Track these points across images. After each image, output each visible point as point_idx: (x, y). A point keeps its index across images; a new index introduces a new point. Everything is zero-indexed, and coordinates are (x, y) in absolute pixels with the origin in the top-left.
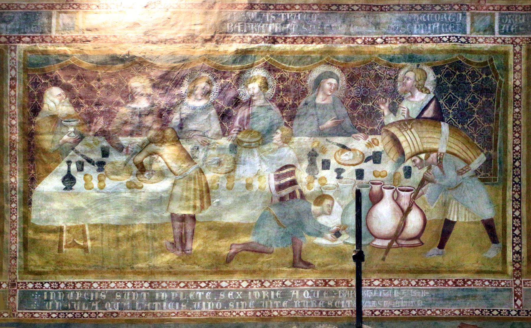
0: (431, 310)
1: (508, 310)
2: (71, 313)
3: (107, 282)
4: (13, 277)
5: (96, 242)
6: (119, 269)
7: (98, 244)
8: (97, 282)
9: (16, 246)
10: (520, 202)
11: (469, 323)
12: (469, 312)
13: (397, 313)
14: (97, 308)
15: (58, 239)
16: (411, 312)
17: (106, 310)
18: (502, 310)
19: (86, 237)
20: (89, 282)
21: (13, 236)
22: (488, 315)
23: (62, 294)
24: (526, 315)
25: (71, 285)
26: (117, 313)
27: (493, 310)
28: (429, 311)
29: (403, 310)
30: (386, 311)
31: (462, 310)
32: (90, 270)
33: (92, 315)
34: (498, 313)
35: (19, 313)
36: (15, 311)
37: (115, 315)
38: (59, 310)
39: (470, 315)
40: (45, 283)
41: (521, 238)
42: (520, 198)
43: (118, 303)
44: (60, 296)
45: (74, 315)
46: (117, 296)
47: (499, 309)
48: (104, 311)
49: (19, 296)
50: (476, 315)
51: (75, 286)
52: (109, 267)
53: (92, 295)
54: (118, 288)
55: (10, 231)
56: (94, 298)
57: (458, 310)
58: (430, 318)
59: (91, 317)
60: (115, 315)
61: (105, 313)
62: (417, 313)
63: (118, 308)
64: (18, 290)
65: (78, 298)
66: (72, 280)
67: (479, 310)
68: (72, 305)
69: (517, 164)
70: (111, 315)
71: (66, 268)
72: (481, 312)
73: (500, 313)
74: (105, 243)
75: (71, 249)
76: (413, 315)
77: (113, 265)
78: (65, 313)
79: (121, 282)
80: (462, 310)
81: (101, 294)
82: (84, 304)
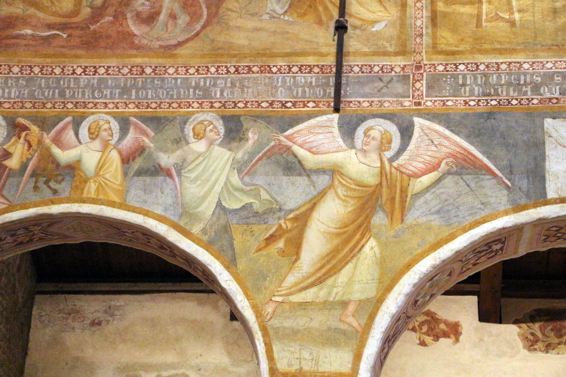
2: (496, 100)
3: (541, 62)
4: (418, 58)
5: (525, 14)
6: (557, 46)
7: (528, 17)
8: (528, 62)
9: (422, 21)
14: (529, 93)
15: (476, 12)
17: (541, 95)
19: (513, 9)
20: (518, 63)
21: (419, 9)
23: (482, 77)
25: (493, 67)
26: (557, 99)
32: (519, 47)
33: (523, 102)
35: (427, 101)
36: (422, 98)
37: (554, 101)
38: (479, 96)
40: (460, 64)
43: (558, 87)
44: (479, 80)
45: (499, 102)
46: (556, 78)
48: (539, 97)
49: (426, 80)
51: (498, 67)
52: (544, 44)
53: (522, 78)
54: (557, 68)
55: (415, 3)
56: (525, 82)
59: (522, 104)
60: (554, 101)
61: (541, 99)
63: (558, 93)
64: (425, 74)
65: (503, 82)
66: (494, 61)
68: (496, 90)
70: (550, 101)
71: (487, 46)
74: (538, 16)
75: (493, 23)
77: (550, 42)
78: (486, 100)
79: (561, 61)
81: (535, 77)
82: (511, 89)
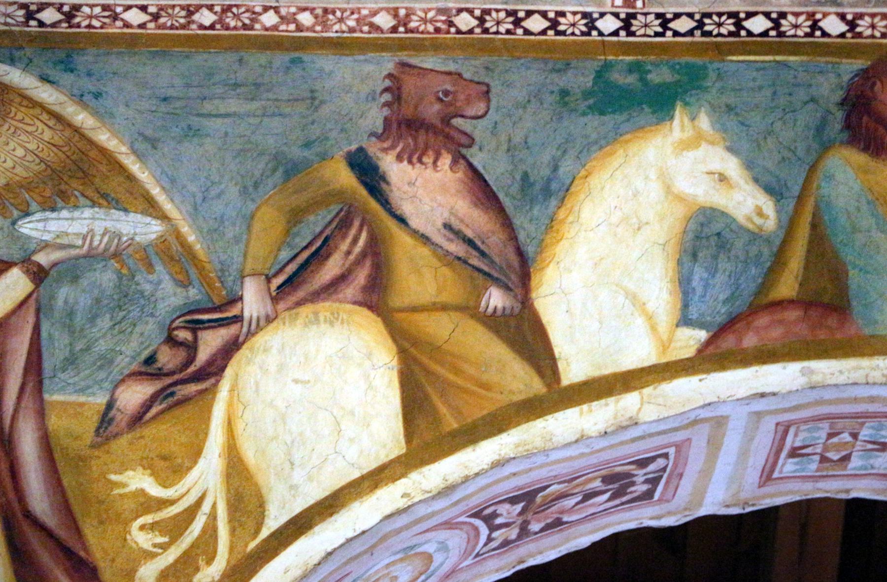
0: (276, 10)
1: (585, 15)
11: (429, 62)
12: (432, 21)
13: (135, 17)
16: (196, 17)
18: (562, 14)
22: (508, 32)
24: (657, 34)
27: (529, 13)
28: (271, 13)
29: (161, 8)
30: (86, 10)
31: (402, 12)
34: (546, 24)
39: (437, 30)
47: (551, 9)
50: (459, 32)
57: (387, 10)
58: (271, 43)
62: (220, 21)
67: (470, 11)
72: (482, 20)
73: (554, 24)
76: (202, 27)
80: (402, 12)
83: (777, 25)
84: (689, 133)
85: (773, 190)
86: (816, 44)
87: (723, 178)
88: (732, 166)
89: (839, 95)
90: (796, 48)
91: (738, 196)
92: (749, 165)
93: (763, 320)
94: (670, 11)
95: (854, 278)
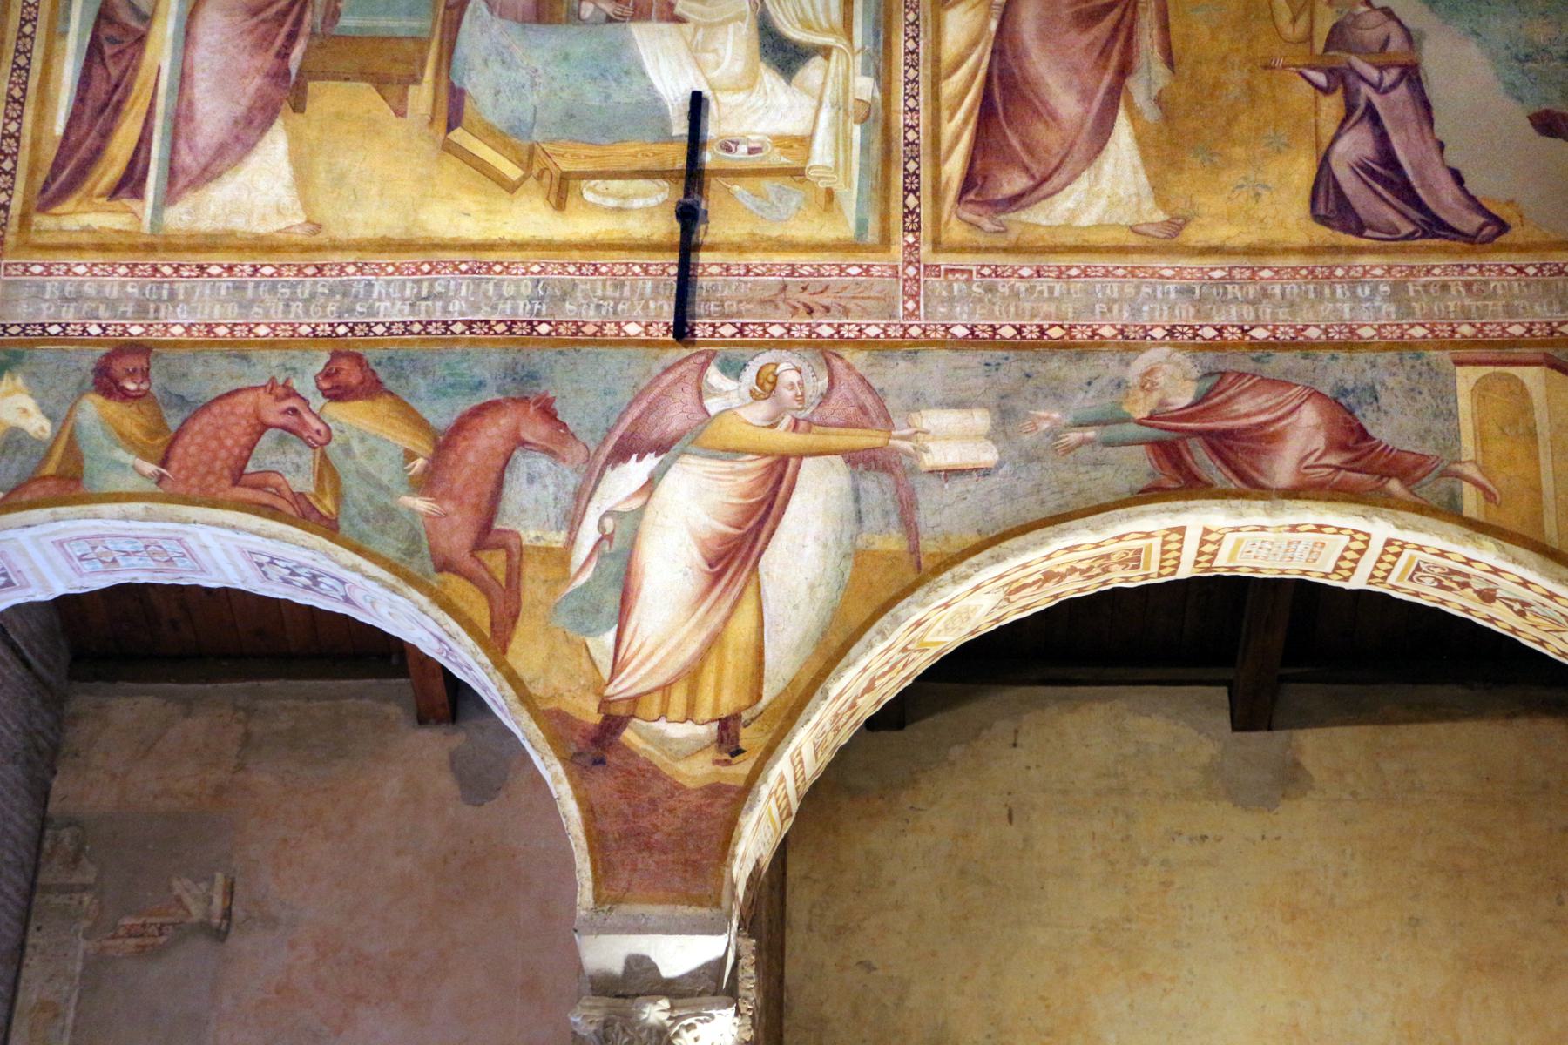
10: (22, 105)
41: (13, 177)
42: (24, 96)
69: (28, 29)
83: (64, 329)
84: (10, 387)
85: (51, 417)
86: (84, 339)
87: (25, 411)
88: (30, 403)
89: (93, 366)
90: (72, 342)
91: (32, 420)
92: (41, 404)
93: (35, 487)
94: (8, 322)
95: (87, 463)
